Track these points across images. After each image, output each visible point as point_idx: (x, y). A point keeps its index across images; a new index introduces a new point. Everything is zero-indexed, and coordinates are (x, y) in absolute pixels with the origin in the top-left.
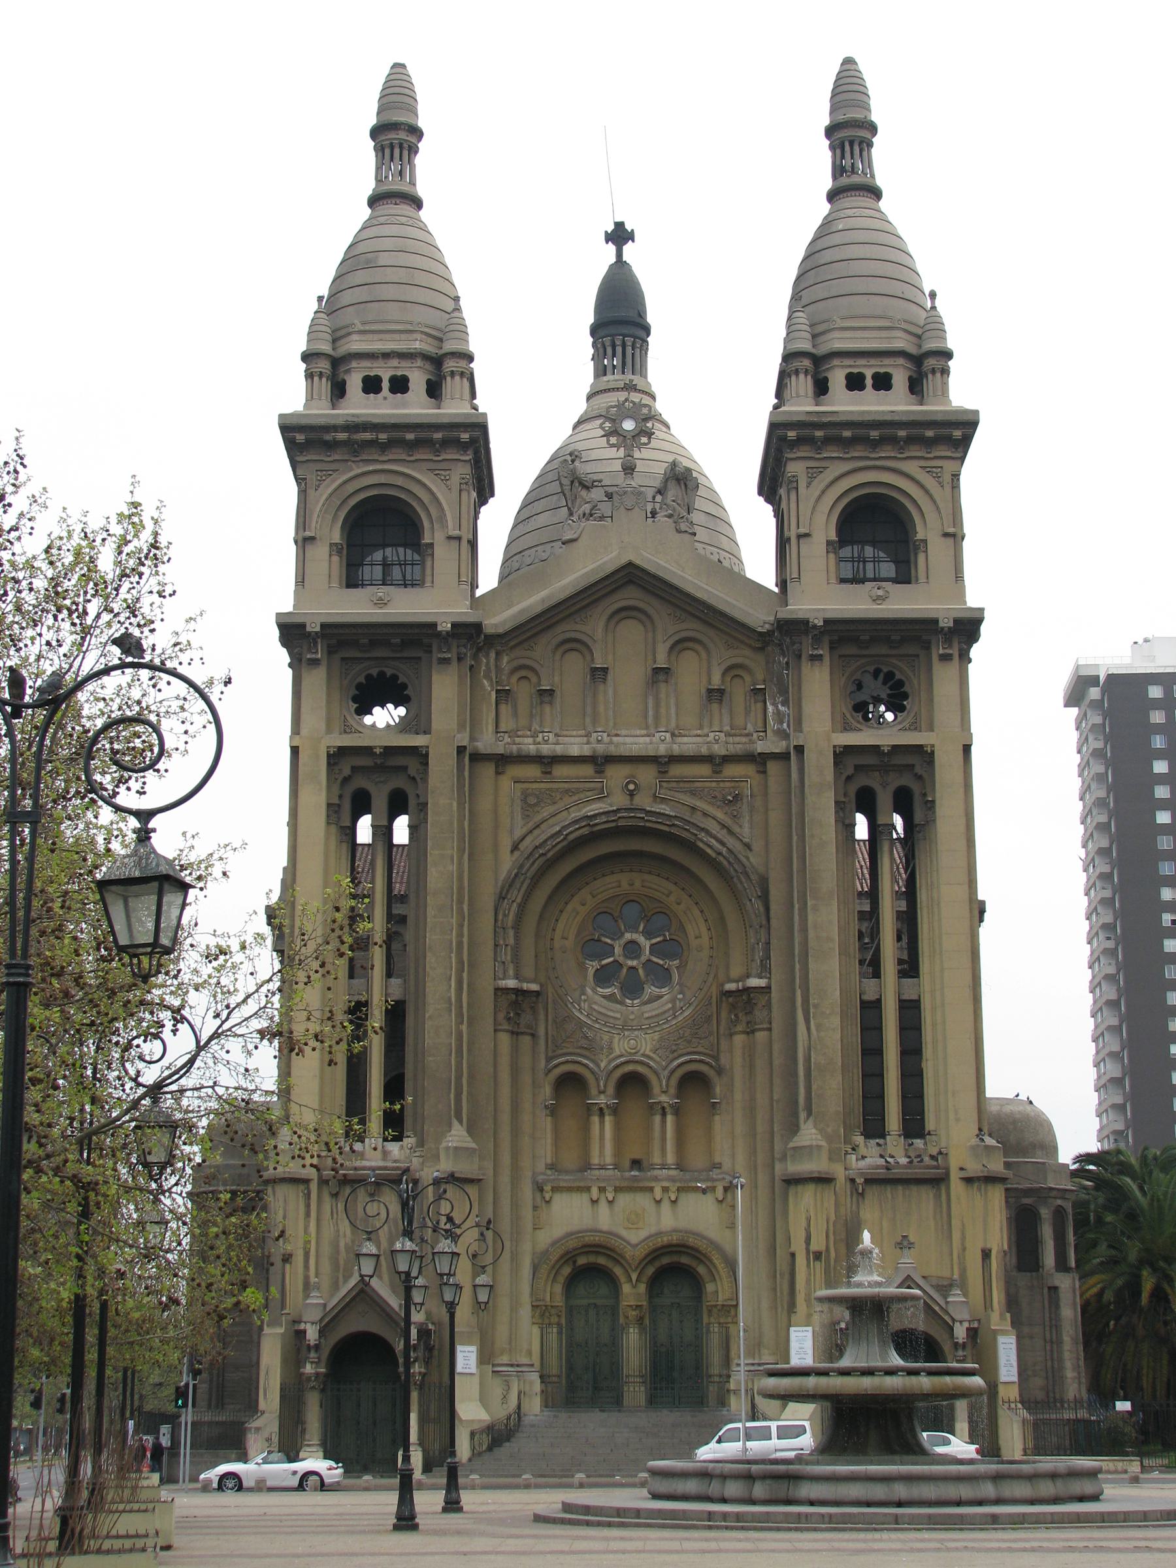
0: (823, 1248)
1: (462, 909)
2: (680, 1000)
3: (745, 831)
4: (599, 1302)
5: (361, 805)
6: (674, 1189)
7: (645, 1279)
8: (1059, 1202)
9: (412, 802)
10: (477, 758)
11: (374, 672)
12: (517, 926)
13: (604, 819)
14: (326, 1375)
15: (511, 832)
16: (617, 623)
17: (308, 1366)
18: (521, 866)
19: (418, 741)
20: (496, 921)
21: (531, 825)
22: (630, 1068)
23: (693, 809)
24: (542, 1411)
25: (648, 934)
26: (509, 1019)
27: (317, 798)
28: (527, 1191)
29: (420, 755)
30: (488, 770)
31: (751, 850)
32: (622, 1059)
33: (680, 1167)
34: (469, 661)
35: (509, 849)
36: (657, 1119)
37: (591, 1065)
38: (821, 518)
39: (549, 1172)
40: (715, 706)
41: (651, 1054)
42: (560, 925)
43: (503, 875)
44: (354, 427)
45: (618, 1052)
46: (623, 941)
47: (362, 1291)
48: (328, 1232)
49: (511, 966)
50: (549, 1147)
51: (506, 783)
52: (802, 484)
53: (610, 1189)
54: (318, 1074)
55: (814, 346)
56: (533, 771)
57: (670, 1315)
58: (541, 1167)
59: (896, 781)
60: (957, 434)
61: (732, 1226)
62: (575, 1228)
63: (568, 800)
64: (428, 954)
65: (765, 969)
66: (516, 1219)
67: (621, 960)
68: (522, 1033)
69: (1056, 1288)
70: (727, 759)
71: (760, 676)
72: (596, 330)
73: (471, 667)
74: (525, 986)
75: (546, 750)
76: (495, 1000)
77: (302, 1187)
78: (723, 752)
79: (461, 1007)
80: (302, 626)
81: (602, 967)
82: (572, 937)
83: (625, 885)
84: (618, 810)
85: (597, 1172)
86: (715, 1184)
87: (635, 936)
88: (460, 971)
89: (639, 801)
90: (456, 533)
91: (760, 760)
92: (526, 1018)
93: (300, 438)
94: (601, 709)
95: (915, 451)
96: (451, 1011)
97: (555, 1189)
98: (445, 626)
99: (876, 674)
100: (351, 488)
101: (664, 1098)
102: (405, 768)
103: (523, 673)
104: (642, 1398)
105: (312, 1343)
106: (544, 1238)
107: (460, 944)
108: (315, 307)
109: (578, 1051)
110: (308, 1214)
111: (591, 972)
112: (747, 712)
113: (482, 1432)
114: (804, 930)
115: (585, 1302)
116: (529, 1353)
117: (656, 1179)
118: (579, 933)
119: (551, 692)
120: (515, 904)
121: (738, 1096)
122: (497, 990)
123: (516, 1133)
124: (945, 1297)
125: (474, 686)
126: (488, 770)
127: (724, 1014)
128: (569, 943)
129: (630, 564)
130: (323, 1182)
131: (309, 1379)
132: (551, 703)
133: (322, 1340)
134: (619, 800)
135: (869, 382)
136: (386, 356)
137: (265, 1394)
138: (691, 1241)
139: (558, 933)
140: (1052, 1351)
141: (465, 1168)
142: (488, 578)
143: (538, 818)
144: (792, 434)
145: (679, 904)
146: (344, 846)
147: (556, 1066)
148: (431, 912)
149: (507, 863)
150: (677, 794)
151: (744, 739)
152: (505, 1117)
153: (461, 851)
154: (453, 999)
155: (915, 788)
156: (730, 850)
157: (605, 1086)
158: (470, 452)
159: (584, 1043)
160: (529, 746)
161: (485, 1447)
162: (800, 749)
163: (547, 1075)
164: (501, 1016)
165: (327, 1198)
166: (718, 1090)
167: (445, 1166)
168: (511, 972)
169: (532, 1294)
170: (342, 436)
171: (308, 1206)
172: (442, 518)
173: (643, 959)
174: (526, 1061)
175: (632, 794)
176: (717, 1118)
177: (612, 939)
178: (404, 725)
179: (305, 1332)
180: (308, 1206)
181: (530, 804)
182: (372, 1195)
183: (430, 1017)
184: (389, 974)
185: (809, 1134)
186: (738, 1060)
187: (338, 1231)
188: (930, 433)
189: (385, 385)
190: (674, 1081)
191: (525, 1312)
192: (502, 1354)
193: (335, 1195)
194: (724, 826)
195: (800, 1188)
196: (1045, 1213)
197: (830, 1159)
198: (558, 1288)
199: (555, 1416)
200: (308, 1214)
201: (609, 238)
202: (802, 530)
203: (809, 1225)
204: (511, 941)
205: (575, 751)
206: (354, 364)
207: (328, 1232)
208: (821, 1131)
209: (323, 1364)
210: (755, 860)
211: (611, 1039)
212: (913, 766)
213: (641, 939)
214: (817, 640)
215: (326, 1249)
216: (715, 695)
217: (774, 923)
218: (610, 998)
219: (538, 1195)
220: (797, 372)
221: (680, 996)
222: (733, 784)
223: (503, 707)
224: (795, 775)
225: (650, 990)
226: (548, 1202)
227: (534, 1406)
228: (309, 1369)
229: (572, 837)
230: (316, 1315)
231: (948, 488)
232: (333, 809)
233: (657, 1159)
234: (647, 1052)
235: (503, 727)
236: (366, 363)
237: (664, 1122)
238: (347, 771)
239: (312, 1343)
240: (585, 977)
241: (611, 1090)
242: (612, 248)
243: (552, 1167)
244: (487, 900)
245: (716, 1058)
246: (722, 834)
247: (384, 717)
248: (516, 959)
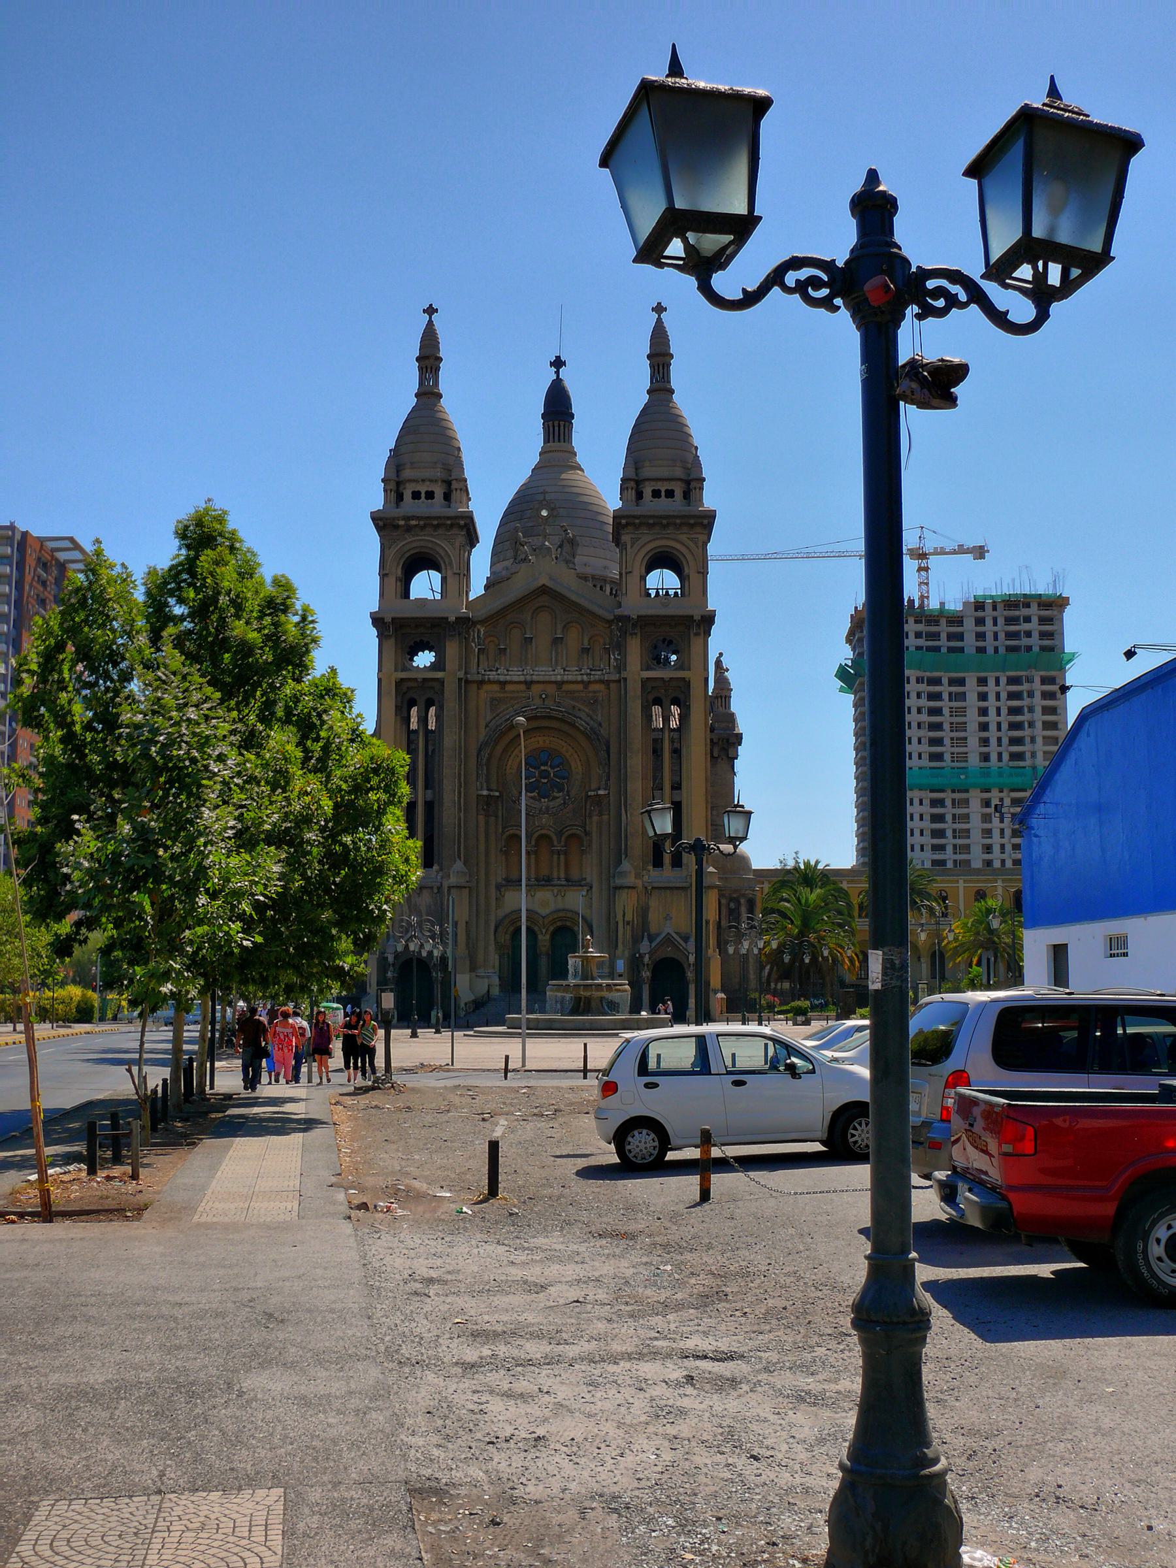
3: (599, 719)
5: (412, 703)
9: (436, 703)
10: (467, 682)
11: (418, 640)
19: (440, 675)
22: (543, 832)
23: (574, 707)
25: (552, 768)
26: (483, 809)
27: (390, 704)
29: (441, 682)
30: (475, 686)
33: (567, 880)
36: (555, 857)
38: (637, 564)
40: (585, 656)
42: (510, 763)
43: (482, 737)
44: (407, 518)
51: (482, 692)
52: (629, 546)
55: (637, 475)
56: (496, 687)
60: (706, 522)
70: (589, 682)
71: (608, 640)
72: (543, 416)
74: (492, 793)
75: (502, 678)
80: (383, 619)
83: (541, 743)
87: (546, 768)
88: (460, 786)
90: (458, 571)
91: (607, 683)
93: (381, 523)
94: (529, 656)
95: (685, 529)
98: (452, 619)
100: (406, 549)
102: (433, 688)
103: (492, 638)
106: (501, 913)
107: (460, 774)
112: (601, 660)
113: (470, 1002)
114: (626, 767)
119: (505, 649)
121: (595, 846)
123: (487, 863)
124: (686, 942)
125: (467, 646)
129: (544, 585)
132: (505, 654)
134: (538, 702)
135: (663, 494)
136: (423, 481)
141: (462, 881)
142: (477, 588)
144: (624, 521)
146: (404, 727)
151: (599, 673)
153: (460, 729)
156: (591, 728)
158: (465, 530)
160: (493, 676)
162: (625, 679)
167: (453, 880)
170: (402, 523)
172: (451, 564)
178: (434, 667)
181: (494, 702)
184: (426, 787)
185: (626, 866)
186: (594, 829)
188: (692, 521)
189: (423, 495)
191: (492, 948)
196: (742, 901)
201: (552, 364)
202: (628, 570)
204: (485, 772)
205: (516, 679)
206: (407, 485)
214: (634, 626)
216: (586, 651)
217: (612, 763)
220: (627, 488)
223: (481, 656)
224: (623, 692)
227: (496, 991)
228: (389, 974)
231: (701, 549)
232: (398, 708)
233: (555, 875)
236: (413, 484)
237: (559, 858)
242: (553, 369)
243: (504, 879)
244: (473, 752)
245: (584, 827)
247: (424, 659)
248: (488, 781)
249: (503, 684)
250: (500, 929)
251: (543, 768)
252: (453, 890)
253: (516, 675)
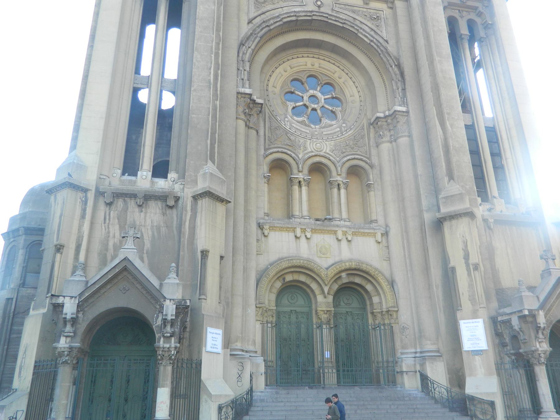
1: (219, 35)
2: (344, 127)
3: (384, 35)
4: (298, 309)
6: (350, 233)
7: (332, 292)
12: (251, 61)
13: (304, 14)
14: (80, 350)
15: (248, 13)
17: (63, 340)
18: (254, 30)
21: (260, 12)
24: (265, 388)
25: (323, 94)
26: (245, 113)
28: (254, 227)
31: (388, 43)
32: (313, 154)
35: (247, 22)
36: (335, 190)
37: (293, 155)
39: (266, 218)
41: (330, 153)
42: (272, 80)
43: (242, 35)
45: (310, 150)
47: (125, 269)
48: (99, 234)
49: (247, 82)
50: (266, 203)
53: (309, 230)
54: (104, 116)
57: (346, 319)
58: (261, 215)
59: (468, 16)
61: (389, 259)
62: (285, 255)
64: (196, 53)
65: (404, 103)
66: (247, 244)
67: (307, 104)
68: (251, 128)
76: (237, 101)
77: (80, 194)
79: (216, 90)
81: (296, 107)
82: (279, 87)
84: (312, 12)
85: (298, 220)
86: (376, 231)
87: (315, 92)
89: (322, 10)
92: (254, 119)
96: (210, 88)
97: (272, 228)
101: (339, 178)
104: (335, 380)
105: (69, 317)
106: (263, 261)
109: (284, 146)
110: (83, 217)
111: (290, 108)
113: (227, 406)
115: (288, 309)
116: (254, 343)
117: (338, 226)
118: (282, 87)
120: (250, 49)
121: (388, 177)
127: (372, 135)
128: (277, 90)
130: (99, 193)
131: (61, 354)
133: (80, 315)
137: (20, 372)
138: (364, 267)
139: (271, 84)
143: (264, 10)
145: (340, 78)
147: (271, 153)
148: (198, 29)
149: (245, 29)
150: (344, 11)
152: (241, 172)
154: (212, 81)
155: (478, 20)
157: (302, 168)
159: (288, 142)
163: (265, 158)
164: (241, 109)
165: (102, 207)
166: (371, 177)
168: (247, 86)
169: (256, 299)
171: (84, 210)
173: (321, 105)
175: (319, 7)
176: (372, 193)
177: (302, 93)
179: (62, 306)
180: (84, 210)
182: (140, 206)
183: (195, 90)
187: (109, 233)
190: (345, 169)
191: (252, 311)
192: (237, 341)
193: (109, 204)
194: (372, 29)
195: (454, 222)
198: (273, 297)
199: (277, 393)
200: (83, 217)
203: (466, 246)
204: (247, 68)
207: (99, 234)
208: (462, 187)
209: (78, 338)
210: (392, 48)
211: (305, 143)
212: (476, 8)
213: (319, 95)
215: (96, 247)
217: (407, 78)
218: (302, 123)
219: (260, 231)
221: (344, 125)
222: (375, 11)
225: (325, 121)
227: (260, 383)
228: (63, 343)
229: (285, 20)
230: (76, 290)
233: (336, 215)
234: (328, 151)
237: (339, 194)
239: (69, 317)
240: (287, 111)
241: (306, 171)
244: (234, 43)
246: (372, 33)
250: (265, 282)
251: (312, 92)
252: (204, 203)
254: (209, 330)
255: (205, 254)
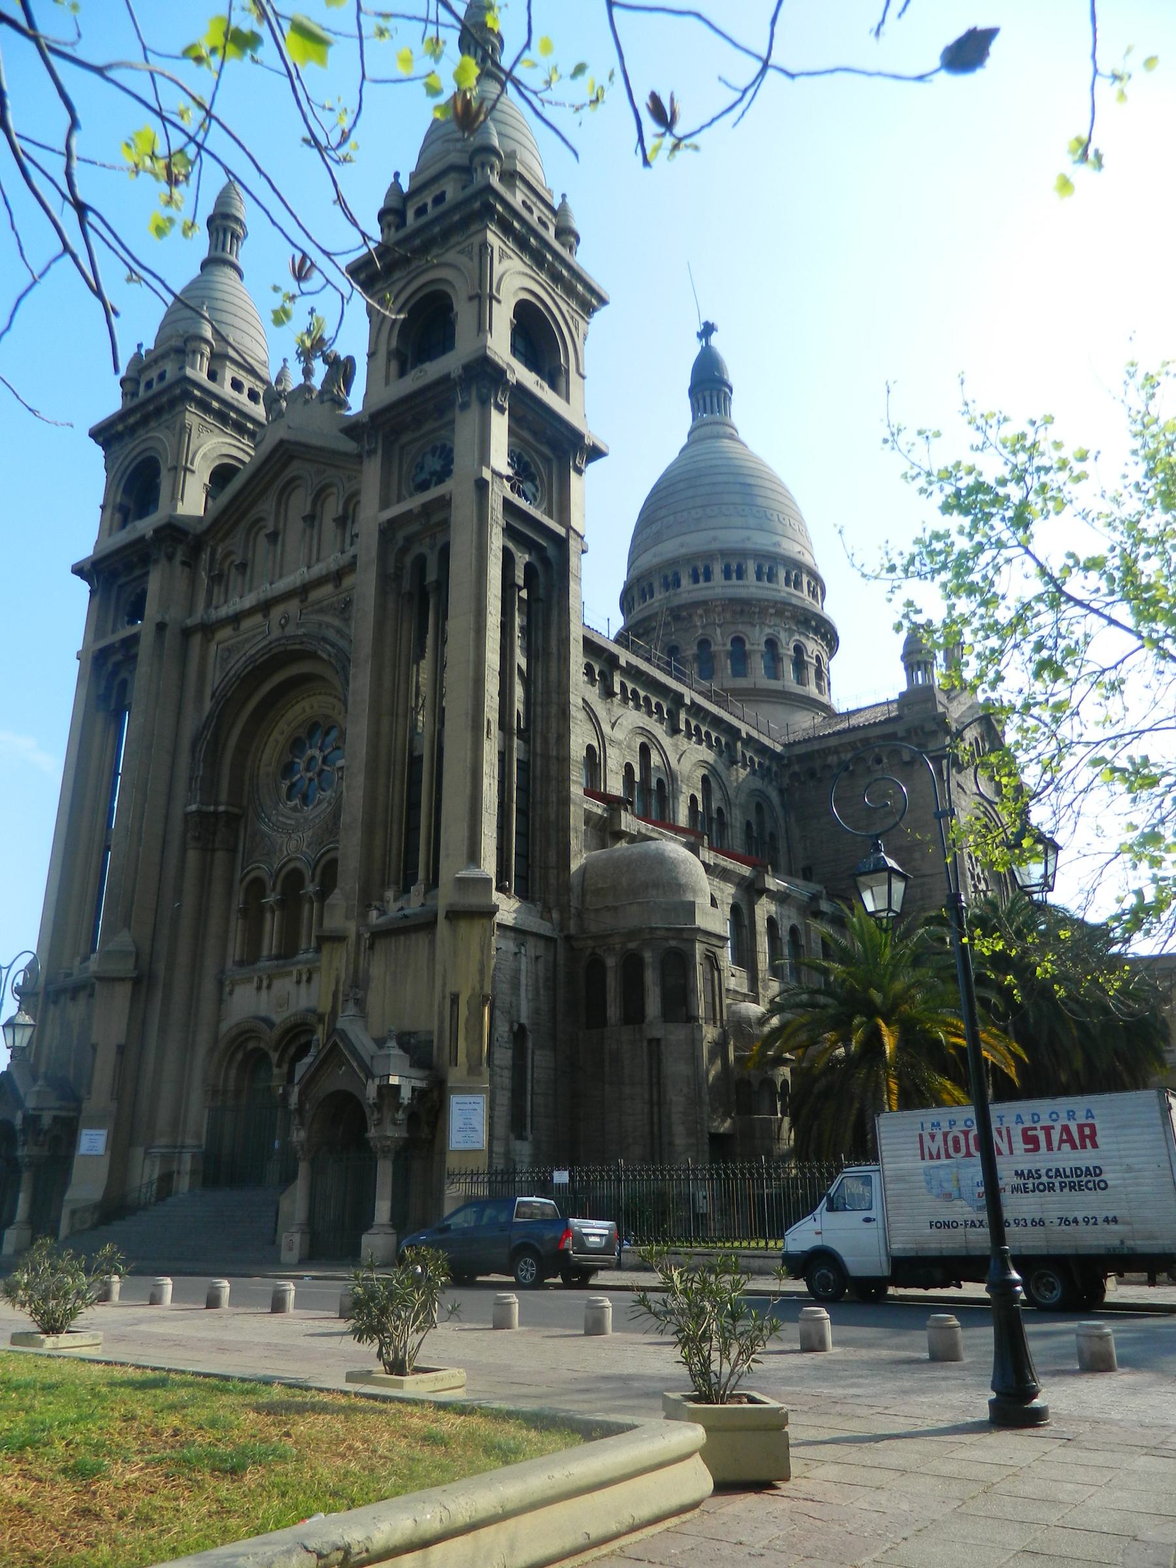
0: (329, 1009)
8: (673, 943)
10: (187, 633)
16: (290, 495)
20: (193, 758)
34: (179, 557)
46: (305, 758)
51: (213, 647)
63: (247, 646)
69: (658, 1040)
73: (183, 563)
78: (337, 567)
83: (308, 709)
98: (150, 534)
99: (433, 453)
100: (126, 463)
106: (224, 1027)
108: (136, 350)
122: (186, 815)
126: (196, 640)
129: (282, 442)
134: (276, 633)
140: (652, 1113)
160: (224, 611)
161: (86, 1226)
170: (120, 427)
173: (317, 769)
174: (218, 871)
175: (283, 627)
196: (648, 956)
197: (347, 918)
226: (231, 993)
235: (214, 602)
238: (110, 666)
249: (236, 619)
253: (249, 601)
254: (85, 1132)
255: (94, 1048)
